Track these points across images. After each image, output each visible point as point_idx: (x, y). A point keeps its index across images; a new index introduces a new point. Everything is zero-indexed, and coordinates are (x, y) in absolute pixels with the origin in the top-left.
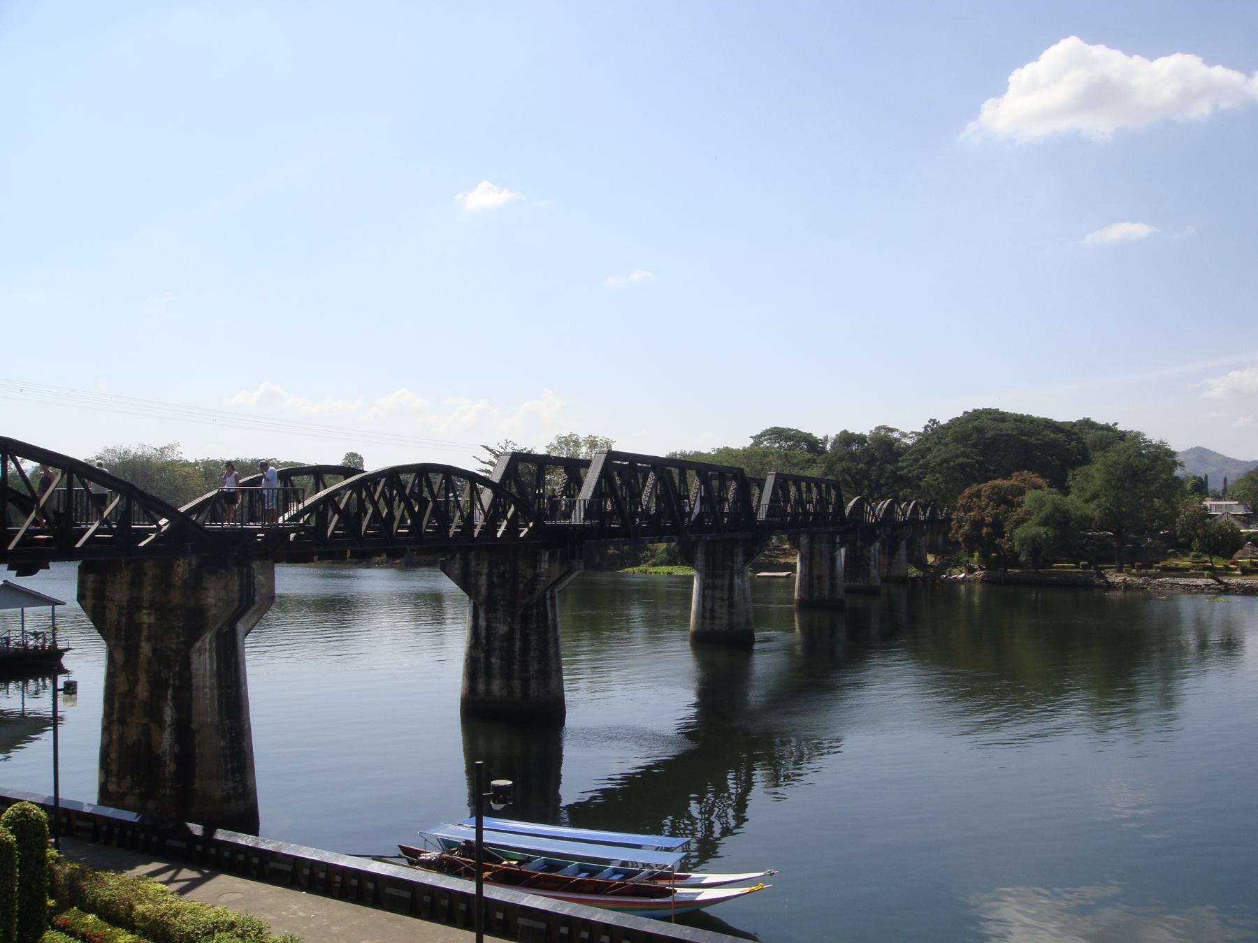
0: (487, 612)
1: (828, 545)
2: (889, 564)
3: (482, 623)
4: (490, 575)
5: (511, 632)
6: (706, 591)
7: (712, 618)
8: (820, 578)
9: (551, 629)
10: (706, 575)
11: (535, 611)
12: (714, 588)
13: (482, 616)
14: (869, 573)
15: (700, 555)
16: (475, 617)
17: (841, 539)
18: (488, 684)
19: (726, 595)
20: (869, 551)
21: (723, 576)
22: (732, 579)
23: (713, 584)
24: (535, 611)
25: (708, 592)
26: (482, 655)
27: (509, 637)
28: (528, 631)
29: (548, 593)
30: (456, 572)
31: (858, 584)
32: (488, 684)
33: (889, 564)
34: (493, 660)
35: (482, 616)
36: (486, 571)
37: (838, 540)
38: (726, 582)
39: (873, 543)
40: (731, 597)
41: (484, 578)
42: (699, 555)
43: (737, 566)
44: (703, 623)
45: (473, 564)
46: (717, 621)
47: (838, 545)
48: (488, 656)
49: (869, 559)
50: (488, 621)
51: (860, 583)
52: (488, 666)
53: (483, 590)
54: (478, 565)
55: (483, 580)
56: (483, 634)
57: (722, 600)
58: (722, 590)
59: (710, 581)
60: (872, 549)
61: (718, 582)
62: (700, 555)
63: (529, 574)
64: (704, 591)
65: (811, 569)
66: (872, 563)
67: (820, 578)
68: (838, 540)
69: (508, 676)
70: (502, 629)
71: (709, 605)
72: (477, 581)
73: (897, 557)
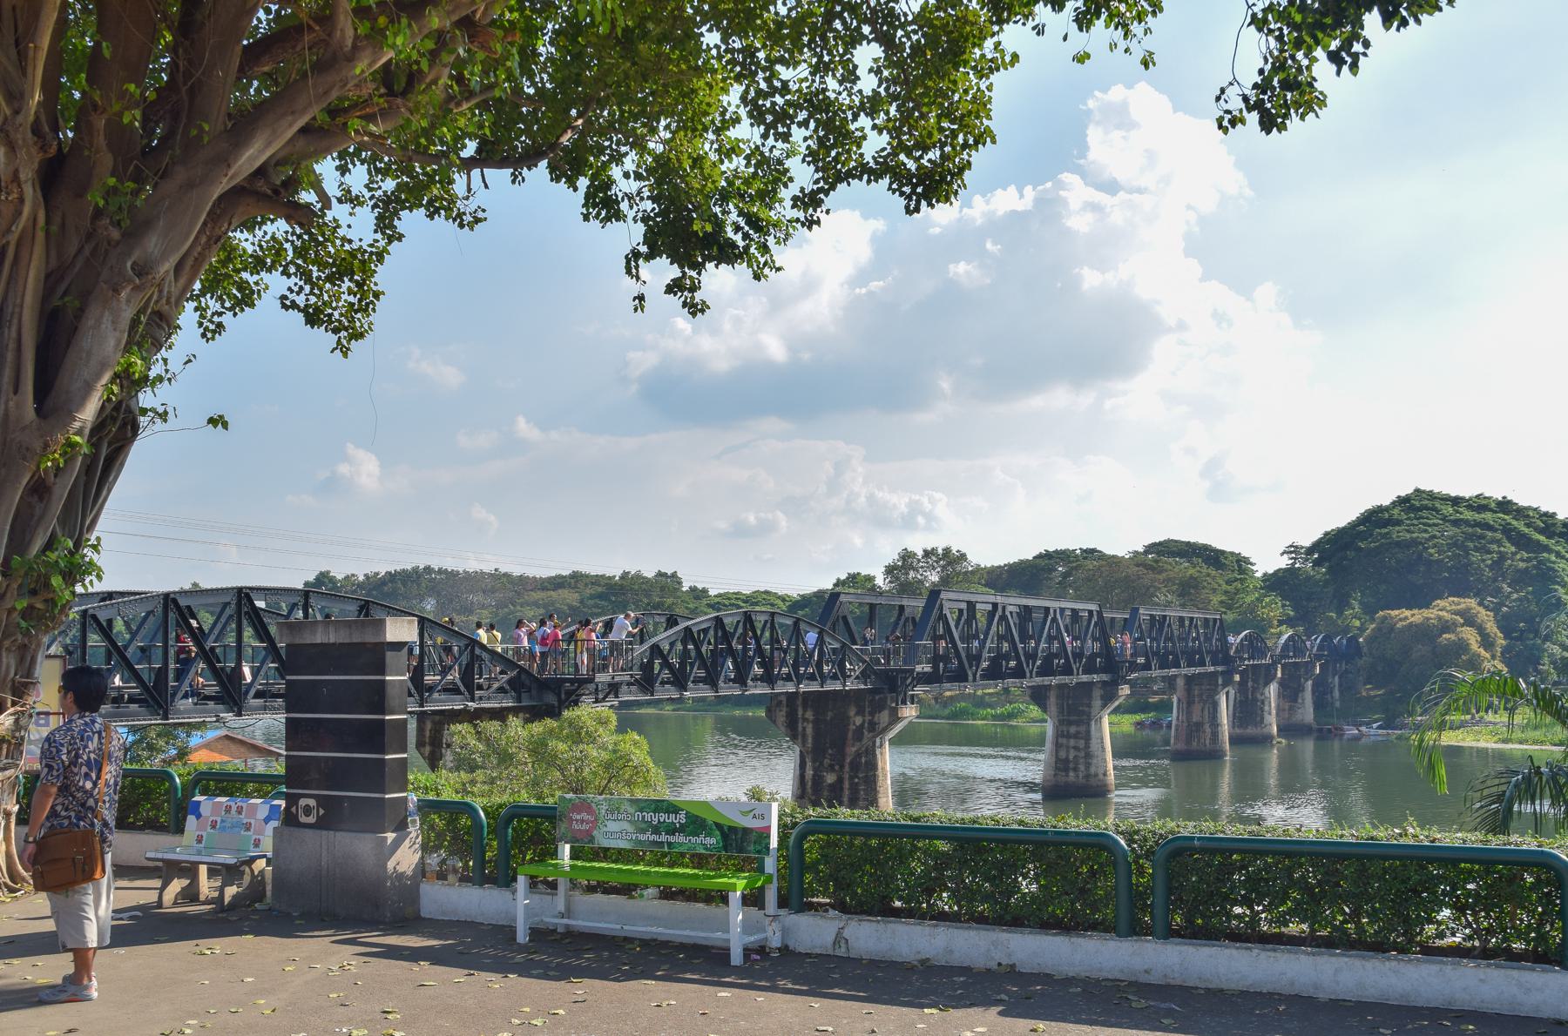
0: (814, 761)
2: (1291, 708)
3: (809, 772)
4: (816, 722)
5: (840, 780)
6: (1060, 740)
7: (1066, 770)
8: (1199, 725)
9: (880, 778)
10: (1059, 721)
11: (863, 760)
12: (1068, 736)
13: (809, 764)
14: (1262, 718)
15: (1052, 700)
19: (1083, 742)
20: (1262, 694)
21: (1078, 723)
22: (1089, 725)
23: (1068, 732)
24: (863, 760)
25: (1064, 741)
28: (856, 780)
29: (878, 740)
30: (783, 719)
35: (809, 764)
36: (811, 718)
37: (1220, 681)
39: (1267, 684)
40: (1087, 746)
41: (810, 725)
43: (1095, 710)
44: (1055, 775)
45: (800, 712)
46: (1071, 774)
47: (1220, 687)
49: (1263, 703)
50: (815, 770)
51: (1251, 731)
53: (810, 740)
54: (805, 711)
55: (809, 730)
56: (810, 783)
57: (1076, 748)
60: (1267, 689)
61: (1073, 729)
62: (1052, 700)
63: (858, 720)
65: (1189, 713)
66: (1266, 708)
67: (1199, 725)
68: (1220, 681)
70: (830, 778)
71: (1063, 754)
72: (804, 729)
73: (1300, 701)
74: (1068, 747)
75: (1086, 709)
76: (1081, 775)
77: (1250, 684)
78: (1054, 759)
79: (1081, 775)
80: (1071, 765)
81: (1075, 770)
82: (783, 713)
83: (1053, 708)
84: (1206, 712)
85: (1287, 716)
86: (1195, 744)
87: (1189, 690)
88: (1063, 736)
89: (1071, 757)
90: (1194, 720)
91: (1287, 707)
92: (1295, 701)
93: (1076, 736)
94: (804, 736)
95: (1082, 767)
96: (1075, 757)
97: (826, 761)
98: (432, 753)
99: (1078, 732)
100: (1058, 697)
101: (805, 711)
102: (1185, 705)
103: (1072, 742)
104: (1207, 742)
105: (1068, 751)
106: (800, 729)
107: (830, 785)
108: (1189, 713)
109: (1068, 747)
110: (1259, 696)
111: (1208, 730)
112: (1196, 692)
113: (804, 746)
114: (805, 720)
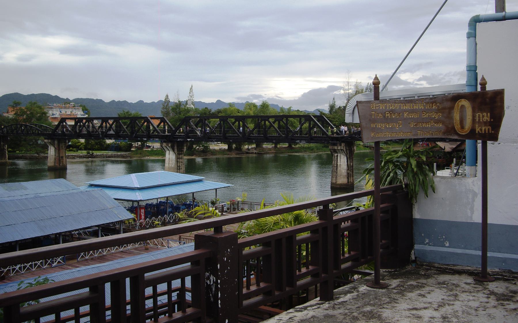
1: (64, 144)
3: (349, 163)
6: (178, 160)
8: (62, 157)
12: (179, 159)
17: (68, 141)
31: (2, 161)
42: (175, 147)
58: (181, 159)
59: (178, 156)
61: (180, 156)
64: (177, 159)
65: (59, 154)
71: (178, 165)
75: (183, 149)
77: (2, 143)
78: (177, 166)
80: (181, 168)
81: (182, 169)
83: (176, 150)
86: (61, 164)
87: (59, 145)
96: (181, 165)
100: (177, 147)
102: (58, 151)
108: (59, 154)
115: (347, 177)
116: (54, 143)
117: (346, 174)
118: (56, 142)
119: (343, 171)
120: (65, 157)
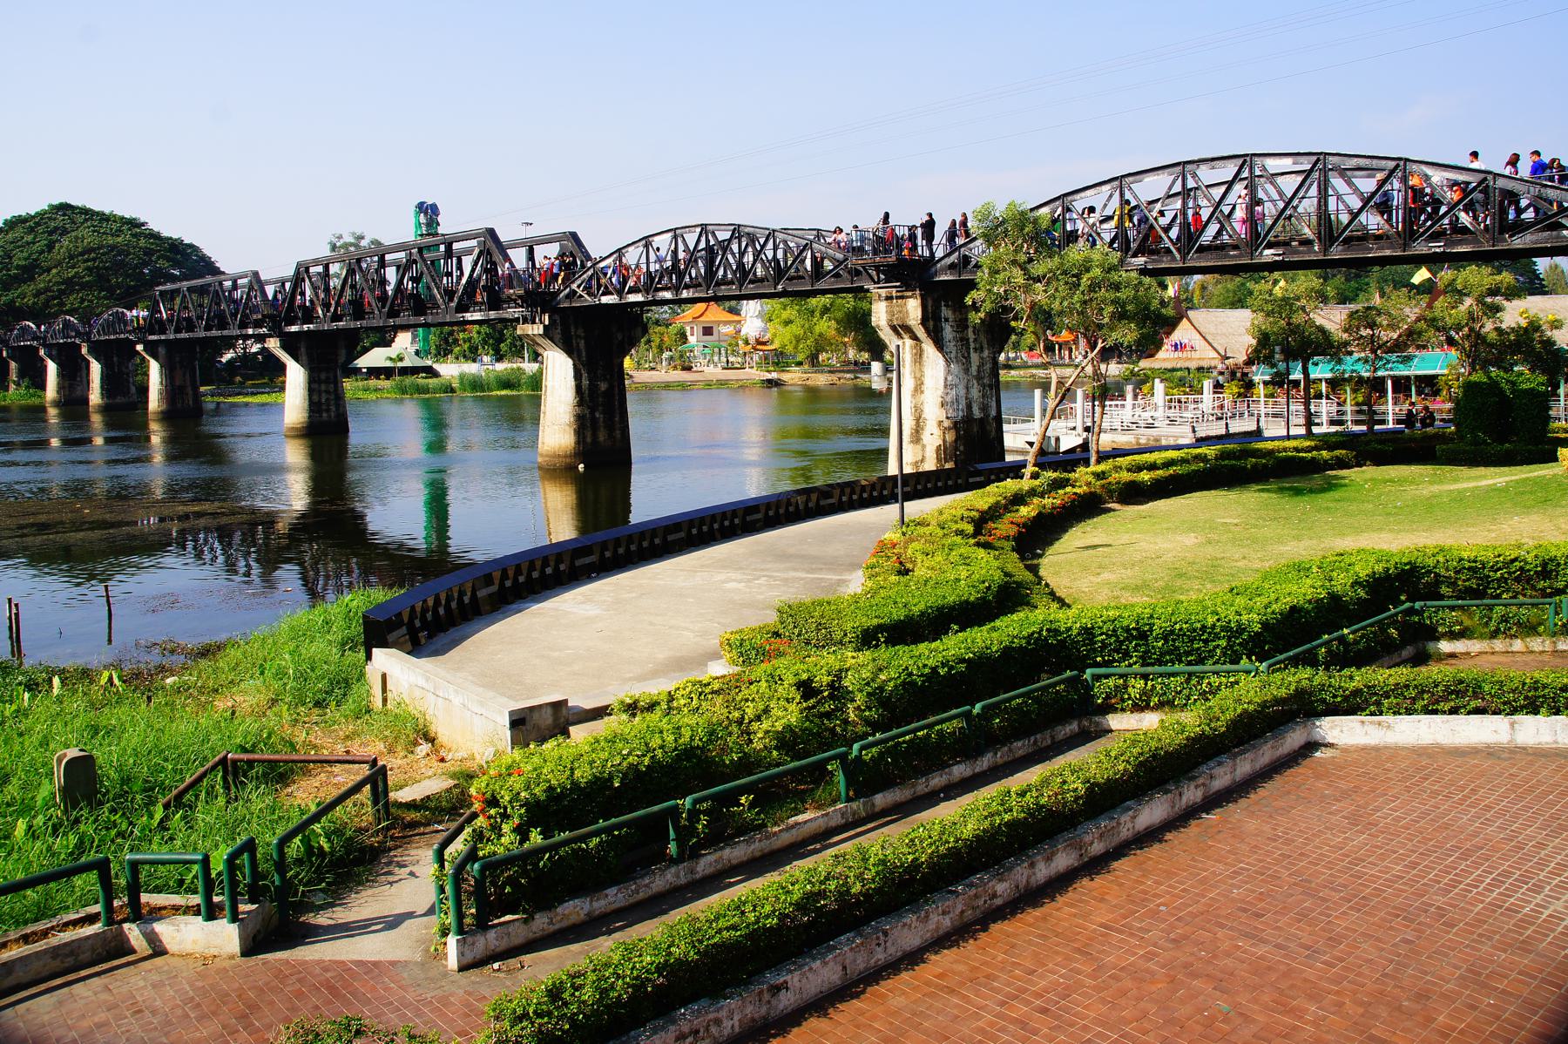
3: (585, 382)
5: (611, 388)
8: (181, 389)
12: (320, 382)
16: (578, 376)
18: (595, 435)
20: (127, 367)
23: (319, 377)
25: (315, 386)
26: (587, 412)
27: (608, 394)
30: (559, 336)
32: (595, 435)
33: (71, 387)
34: (597, 415)
35: (585, 375)
38: (331, 375)
44: (310, 417)
46: (325, 415)
48: (592, 413)
51: (119, 400)
52: (594, 421)
53: (584, 354)
57: (328, 392)
61: (323, 376)
67: (181, 389)
69: (610, 428)
70: (603, 386)
71: (315, 398)
72: (578, 344)
74: (320, 393)
76: (333, 414)
77: (115, 359)
79: (333, 414)
80: (324, 407)
81: (328, 411)
82: (559, 331)
84: (188, 375)
85: (67, 393)
86: (179, 405)
88: (315, 382)
89: (323, 400)
90: (177, 384)
91: (66, 384)
92: (75, 380)
93: (327, 381)
94: (579, 351)
95: (333, 408)
96: (327, 399)
97: (599, 371)
98: (935, 326)
99: (328, 378)
101: (576, 328)
103: (323, 387)
104: (191, 402)
105: (320, 395)
106: (575, 345)
107: (604, 392)
109: (320, 393)
110: (124, 369)
111: (191, 392)
112: (177, 359)
113: (579, 360)
114: (578, 337)
115: (575, 430)
116: (157, 352)
117: (572, 419)
118: (162, 351)
119: (562, 411)
120: (190, 388)
